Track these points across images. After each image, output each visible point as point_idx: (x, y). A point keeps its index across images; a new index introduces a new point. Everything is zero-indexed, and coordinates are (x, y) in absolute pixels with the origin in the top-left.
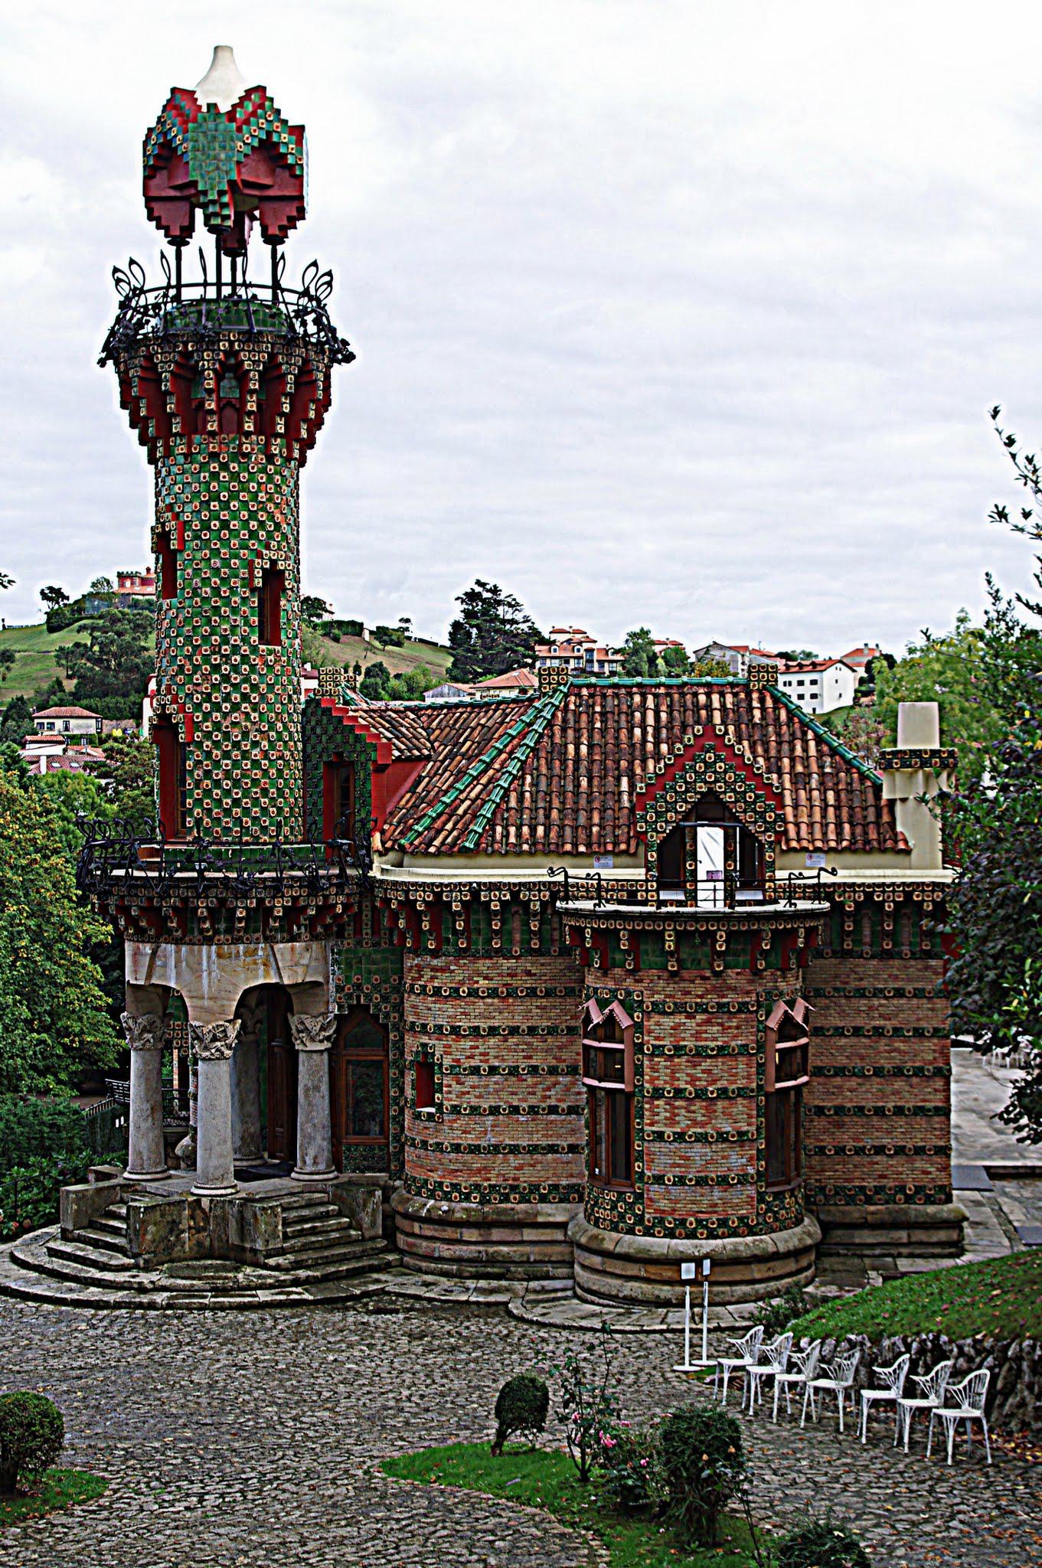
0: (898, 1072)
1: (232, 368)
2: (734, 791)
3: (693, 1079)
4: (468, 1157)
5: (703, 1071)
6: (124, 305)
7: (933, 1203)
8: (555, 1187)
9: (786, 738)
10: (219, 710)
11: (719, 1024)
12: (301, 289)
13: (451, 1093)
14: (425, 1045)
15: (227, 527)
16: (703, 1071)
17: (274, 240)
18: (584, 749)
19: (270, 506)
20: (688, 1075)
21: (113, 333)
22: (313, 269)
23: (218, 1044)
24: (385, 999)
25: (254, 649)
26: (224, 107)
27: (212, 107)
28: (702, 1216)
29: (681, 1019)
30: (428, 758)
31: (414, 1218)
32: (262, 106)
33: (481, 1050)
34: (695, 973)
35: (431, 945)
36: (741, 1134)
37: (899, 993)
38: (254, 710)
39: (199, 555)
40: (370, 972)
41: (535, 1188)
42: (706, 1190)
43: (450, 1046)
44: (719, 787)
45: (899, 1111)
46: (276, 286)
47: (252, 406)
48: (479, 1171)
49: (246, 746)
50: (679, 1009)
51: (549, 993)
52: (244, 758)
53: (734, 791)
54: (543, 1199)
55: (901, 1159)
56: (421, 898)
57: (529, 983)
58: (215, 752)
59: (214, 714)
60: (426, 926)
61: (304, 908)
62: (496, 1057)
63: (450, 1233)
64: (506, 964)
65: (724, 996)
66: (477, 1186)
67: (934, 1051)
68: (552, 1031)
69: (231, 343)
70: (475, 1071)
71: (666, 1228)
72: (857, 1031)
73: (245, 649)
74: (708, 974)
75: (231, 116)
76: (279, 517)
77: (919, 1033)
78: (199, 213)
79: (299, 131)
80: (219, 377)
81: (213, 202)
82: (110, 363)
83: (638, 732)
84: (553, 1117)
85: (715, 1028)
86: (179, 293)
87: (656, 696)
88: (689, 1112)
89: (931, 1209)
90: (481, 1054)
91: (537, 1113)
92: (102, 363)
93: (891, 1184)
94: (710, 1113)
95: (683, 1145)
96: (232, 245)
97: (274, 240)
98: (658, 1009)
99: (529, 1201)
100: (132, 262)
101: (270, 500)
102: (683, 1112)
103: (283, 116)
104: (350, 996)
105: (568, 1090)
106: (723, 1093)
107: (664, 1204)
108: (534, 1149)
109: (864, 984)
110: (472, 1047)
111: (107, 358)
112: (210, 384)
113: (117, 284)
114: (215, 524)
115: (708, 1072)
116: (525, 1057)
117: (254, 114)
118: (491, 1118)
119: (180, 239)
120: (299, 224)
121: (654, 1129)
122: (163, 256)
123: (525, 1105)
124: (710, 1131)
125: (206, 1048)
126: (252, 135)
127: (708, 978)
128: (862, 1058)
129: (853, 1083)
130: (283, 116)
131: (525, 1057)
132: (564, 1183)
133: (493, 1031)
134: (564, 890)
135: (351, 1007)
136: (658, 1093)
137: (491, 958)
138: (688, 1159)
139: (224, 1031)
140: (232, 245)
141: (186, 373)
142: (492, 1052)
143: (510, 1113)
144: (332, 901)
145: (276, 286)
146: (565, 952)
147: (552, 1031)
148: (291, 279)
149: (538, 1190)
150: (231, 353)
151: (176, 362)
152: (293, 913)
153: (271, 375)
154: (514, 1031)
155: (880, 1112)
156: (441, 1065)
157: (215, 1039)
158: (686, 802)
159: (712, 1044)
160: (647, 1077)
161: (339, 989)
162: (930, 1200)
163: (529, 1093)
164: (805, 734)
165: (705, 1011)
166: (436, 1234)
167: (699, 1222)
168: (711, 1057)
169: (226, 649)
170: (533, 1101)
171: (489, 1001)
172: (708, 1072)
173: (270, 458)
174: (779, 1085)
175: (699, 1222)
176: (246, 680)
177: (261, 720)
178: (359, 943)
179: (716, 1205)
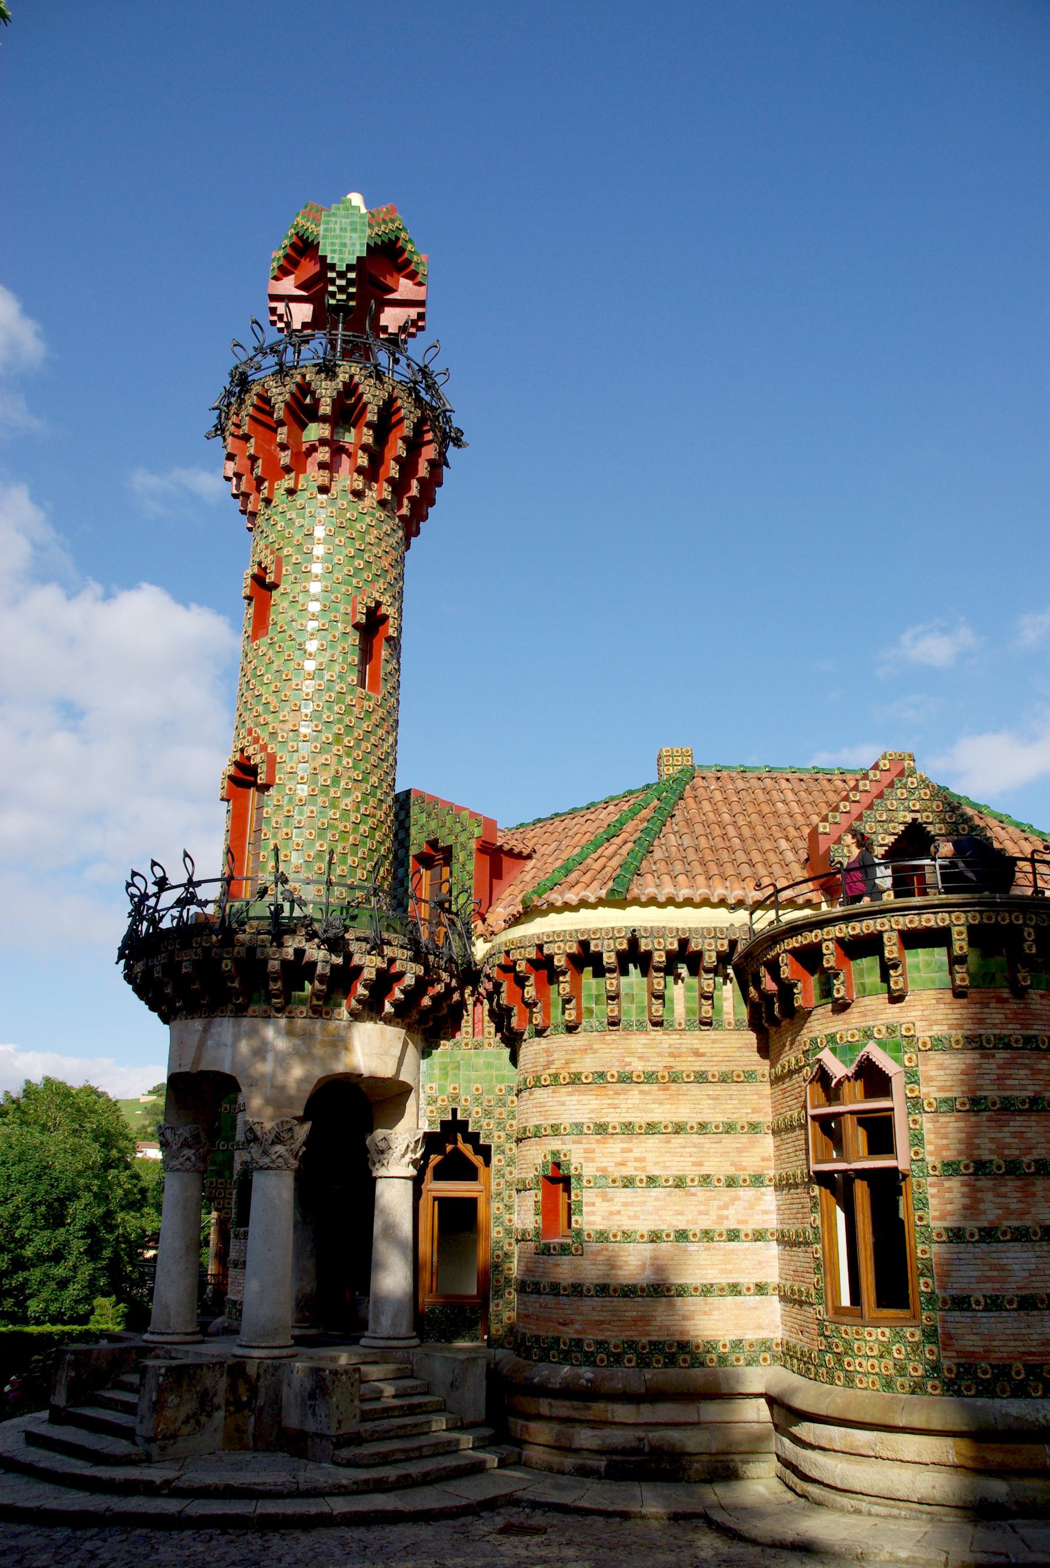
3: (1001, 1147)
5: (1014, 1134)
11: (1025, 1066)
14: (555, 1153)
16: (1014, 1134)
20: (992, 1139)
23: (280, 1149)
24: (488, 1113)
30: (529, 857)
31: (543, 1391)
33: (636, 1153)
38: (348, 755)
40: (469, 1081)
43: (593, 1151)
48: (635, 1321)
56: (560, 955)
57: (698, 1065)
61: (401, 975)
62: (656, 1163)
65: (1026, 1026)
66: (632, 1344)
68: (729, 1128)
70: (628, 1182)
71: (980, 1382)
74: (1006, 994)
81: (341, 275)
85: (1022, 1072)
88: (999, 1196)
90: (637, 1160)
94: (1027, 1194)
95: (995, 1246)
102: (989, 1196)
104: (443, 1110)
105: (751, 1207)
110: (623, 1151)
115: (1018, 1135)
116: (694, 1164)
123: (697, 1228)
124: (1029, 1224)
125: (265, 1153)
127: (1004, 1001)
131: (694, 1164)
133: (651, 1128)
137: (647, 1032)
138: (1002, 1268)
139: (291, 1129)
142: (651, 1157)
154: (679, 1129)
156: (579, 1177)
157: (278, 1140)
163: (700, 1213)
165: (1007, 1046)
166: (575, 1414)
168: (1021, 1112)
170: (706, 1223)
171: (645, 1087)
172: (1018, 1135)
175: (1030, 1369)
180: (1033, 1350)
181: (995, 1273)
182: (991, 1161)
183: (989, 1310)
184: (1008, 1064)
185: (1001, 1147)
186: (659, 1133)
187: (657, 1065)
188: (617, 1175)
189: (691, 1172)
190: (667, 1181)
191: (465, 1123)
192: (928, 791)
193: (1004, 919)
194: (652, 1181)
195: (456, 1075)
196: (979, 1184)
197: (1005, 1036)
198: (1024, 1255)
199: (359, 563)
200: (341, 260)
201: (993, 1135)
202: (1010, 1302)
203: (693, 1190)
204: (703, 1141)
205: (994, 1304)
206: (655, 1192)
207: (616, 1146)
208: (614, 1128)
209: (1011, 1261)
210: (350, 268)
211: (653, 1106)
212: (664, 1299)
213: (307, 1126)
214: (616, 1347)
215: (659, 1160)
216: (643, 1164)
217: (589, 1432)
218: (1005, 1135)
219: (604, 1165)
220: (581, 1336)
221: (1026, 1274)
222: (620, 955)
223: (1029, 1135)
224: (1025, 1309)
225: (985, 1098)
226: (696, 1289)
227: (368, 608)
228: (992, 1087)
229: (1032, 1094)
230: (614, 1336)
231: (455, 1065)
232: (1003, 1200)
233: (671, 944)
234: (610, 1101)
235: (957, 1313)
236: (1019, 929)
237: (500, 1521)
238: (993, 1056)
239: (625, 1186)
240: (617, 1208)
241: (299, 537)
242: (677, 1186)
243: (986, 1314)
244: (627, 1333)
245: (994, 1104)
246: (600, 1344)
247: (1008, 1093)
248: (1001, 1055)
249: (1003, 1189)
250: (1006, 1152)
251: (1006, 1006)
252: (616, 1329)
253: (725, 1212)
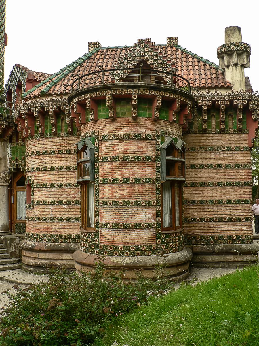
0: (229, 184)
2: (153, 59)
3: (122, 174)
4: (42, 223)
5: (128, 169)
7: (244, 243)
11: (136, 145)
13: (38, 195)
28: (127, 245)
29: (116, 142)
34: (124, 119)
36: (148, 202)
37: (229, 149)
41: (69, 237)
42: (129, 231)
48: (47, 229)
50: (117, 137)
53: (153, 59)
55: (230, 223)
62: (54, 180)
63: (35, 255)
64: (58, 140)
65: (138, 131)
66: (46, 235)
67: (245, 175)
70: (45, 186)
72: (210, 166)
77: (238, 167)
89: (244, 246)
90: (48, 179)
93: (226, 235)
98: (105, 139)
104: (14, 165)
106: (138, 181)
107: (108, 238)
108: (69, 220)
109: (212, 145)
115: (130, 170)
118: (52, 206)
121: (103, 200)
123: (65, 200)
124: (131, 200)
128: (212, 178)
129: (208, 189)
133: (52, 169)
136: (105, 181)
142: (52, 178)
143: (59, 204)
149: (71, 237)
154: (61, 169)
156: (33, 184)
159: (132, 155)
160: (100, 174)
161: (10, 162)
165: (129, 138)
167: (126, 248)
168: (131, 161)
170: (69, 198)
171: (52, 156)
172: (130, 170)
174: (168, 178)
178: (17, 144)
179: (134, 239)
180: (128, 241)
181: (117, 216)
182: (119, 178)
183: (114, 228)
184: (128, 144)
185: (122, 174)
186: (55, 170)
187: (55, 148)
188: (42, 183)
189: (65, 182)
190: (57, 185)
191: (20, 168)
192: (148, 48)
193: (125, 92)
194: (52, 185)
195: (17, 154)
196: (114, 186)
197: (128, 135)
198: (127, 210)
201: (120, 169)
202: (121, 226)
203: (65, 188)
204: (69, 172)
205: (116, 226)
206: (53, 189)
207: (42, 174)
208: (41, 169)
209: (123, 212)
211: (53, 161)
212: (56, 222)
214: (41, 236)
215: (55, 178)
216: (50, 180)
217: (33, 260)
218: (124, 170)
219: (39, 180)
220: (34, 233)
221: (128, 217)
222: (39, 112)
223: (134, 169)
224: (126, 228)
225: (118, 156)
226: (65, 219)
228: (121, 153)
229: (136, 155)
230: (41, 233)
231: (17, 151)
232: (122, 192)
233: (55, 108)
234: (41, 160)
235: (105, 229)
238: (123, 142)
239: (44, 187)
240: (42, 194)
242: (60, 187)
243: (113, 230)
244: (45, 232)
245: (121, 158)
246: (37, 235)
247: (127, 155)
248: (126, 141)
249: (122, 188)
250: (124, 175)
251: (130, 123)
252: (42, 231)
253: (75, 195)
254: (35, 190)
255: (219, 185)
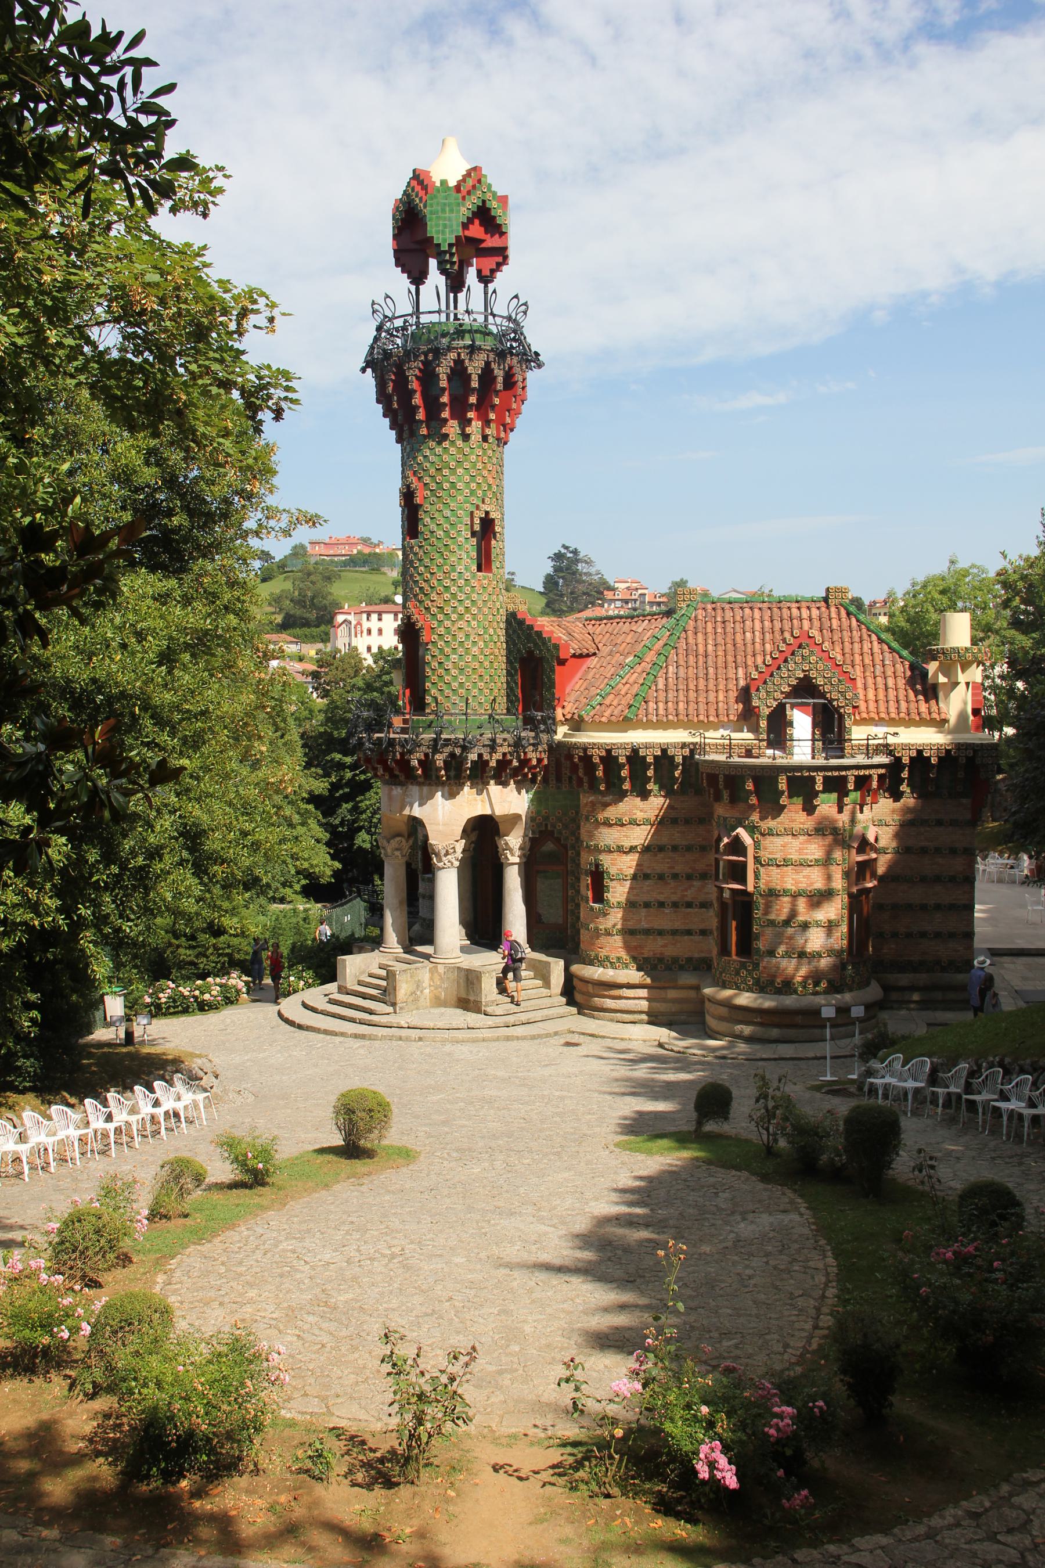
0: (938, 879)
1: (459, 372)
3: (797, 882)
5: (804, 877)
6: (379, 329)
7: (960, 972)
8: (689, 960)
9: (857, 639)
10: (449, 619)
12: (506, 314)
15: (455, 487)
17: (485, 279)
18: (710, 648)
19: (485, 473)
21: (372, 347)
22: (515, 300)
24: (565, 826)
25: (474, 576)
26: (452, 183)
27: (444, 183)
29: (789, 839)
30: (594, 654)
32: (479, 181)
35: (602, 788)
38: (474, 619)
39: (434, 508)
41: (675, 960)
44: (813, 674)
45: (938, 907)
46: (488, 311)
47: (473, 400)
49: (468, 644)
51: (687, 822)
52: (467, 654)
54: (682, 968)
56: (596, 755)
58: (446, 649)
59: (446, 622)
60: (600, 773)
68: (689, 848)
69: (459, 354)
73: (467, 575)
75: (458, 188)
76: (491, 481)
78: (433, 263)
79: (504, 200)
80: (450, 379)
82: (369, 370)
83: (748, 635)
84: (689, 910)
86: (418, 318)
87: (760, 609)
91: (677, 907)
92: (363, 370)
96: (456, 284)
97: (485, 279)
98: (770, 833)
99: (671, 969)
100: (387, 296)
101: (484, 468)
103: (493, 189)
108: (674, 932)
111: (367, 366)
112: (443, 384)
113: (374, 312)
114: (446, 485)
115: (808, 877)
117: (474, 187)
119: (418, 277)
120: (504, 268)
122: (410, 292)
126: (471, 203)
130: (493, 189)
132: (696, 955)
134: (700, 748)
135: (541, 832)
140: (456, 284)
141: (428, 377)
144: (529, 756)
145: (488, 311)
146: (699, 792)
147: (689, 848)
148: (500, 307)
150: (459, 362)
151: (420, 369)
152: (503, 764)
153: (487, 375)
155: (924, 908)
157: (447, 854)
158: (789, 685)
159: (811, 857)
162: (959, 971)
164: (870, 636)
169: (454, 575)
170: (675, 898)
172: (808, 877)
173: (485, 438)
176: (467, 598)
177: (479, 627)
191: (552, 832)
199: (473, 485)
200: (445, 240)
206: (648, 883)
210: (450, 245)
213: (464, 841)
218: (800, 877)
227: (481, 519)
236: (814, 778)
237: (563, 1041)
241: (432, 471)
248: (802, 838)
254: (612, 884)
255: (923, 879)
